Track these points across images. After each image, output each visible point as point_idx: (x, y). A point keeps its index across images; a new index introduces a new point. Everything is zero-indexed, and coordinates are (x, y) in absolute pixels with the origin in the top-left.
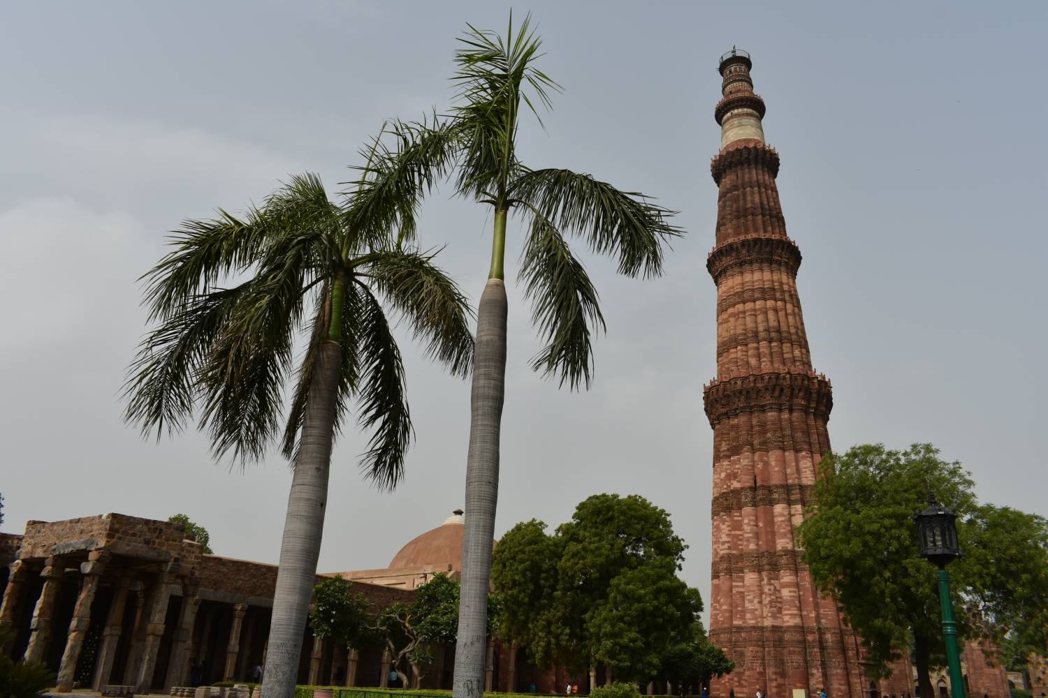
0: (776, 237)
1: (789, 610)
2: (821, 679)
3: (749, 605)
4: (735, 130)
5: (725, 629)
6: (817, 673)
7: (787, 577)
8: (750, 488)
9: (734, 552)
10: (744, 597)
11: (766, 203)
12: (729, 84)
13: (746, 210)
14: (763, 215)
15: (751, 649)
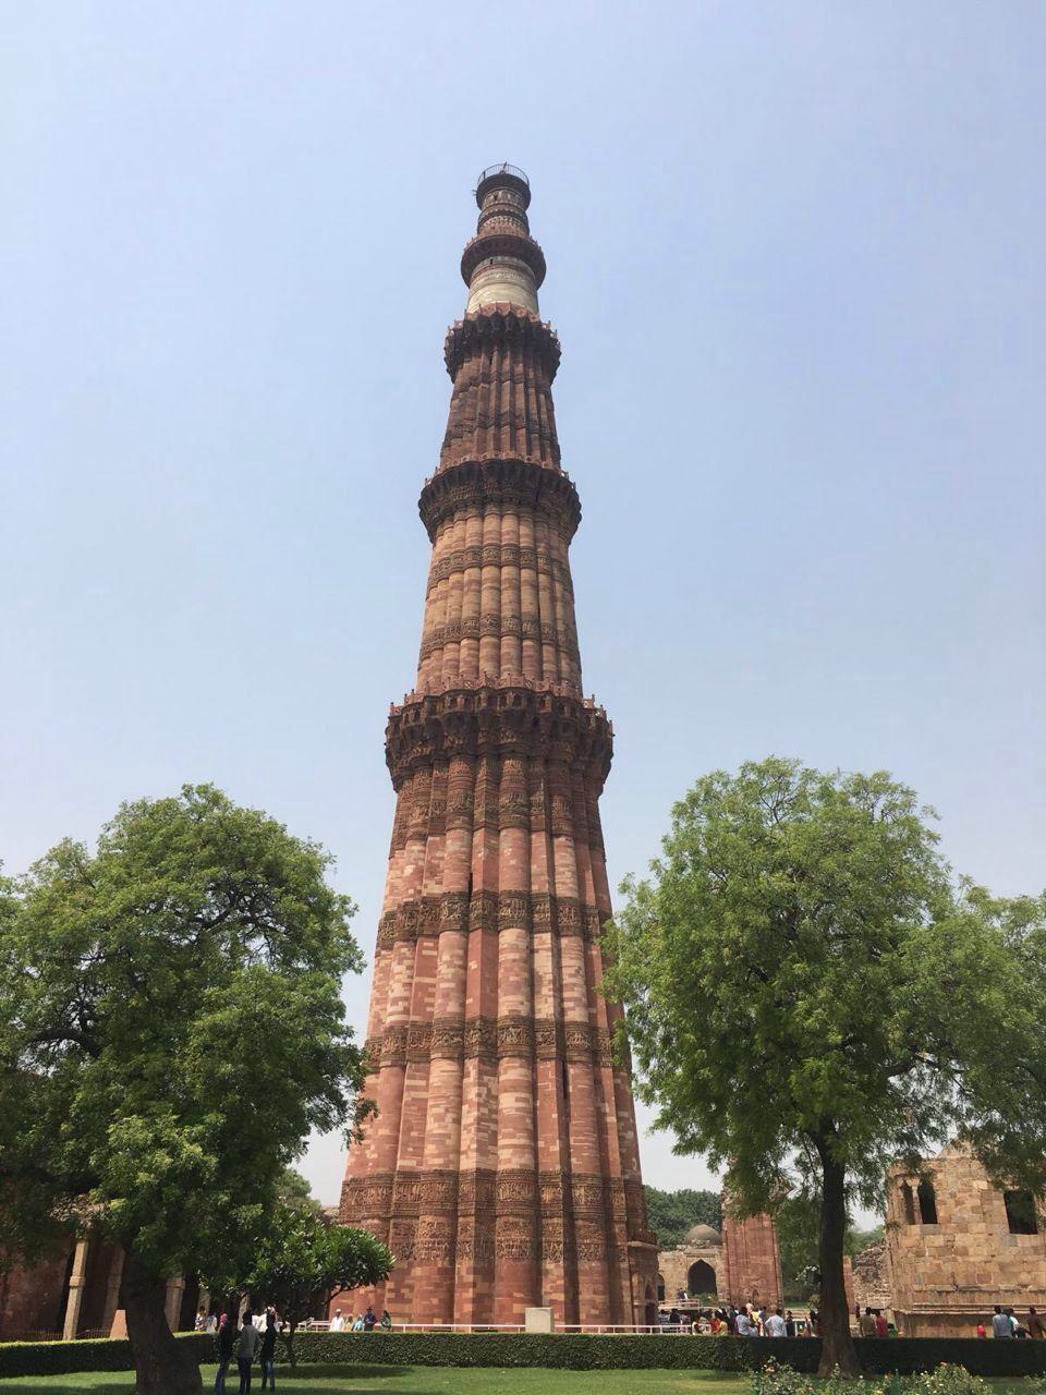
0: (547, 464)
1: (512, 1136)
2: (562, 1282)
3: (436, 1125)
4: (494, 289)
5: (379, 1177)
6: (554, 1269)
7: (512, 1071)
8: (461, 894)
9: (413, 1018)
10: (423, 1111)
11: (535, 411)
12: (492, 215)
13: (499, 416)
14: (529, 432)
15: (429, 1219)
